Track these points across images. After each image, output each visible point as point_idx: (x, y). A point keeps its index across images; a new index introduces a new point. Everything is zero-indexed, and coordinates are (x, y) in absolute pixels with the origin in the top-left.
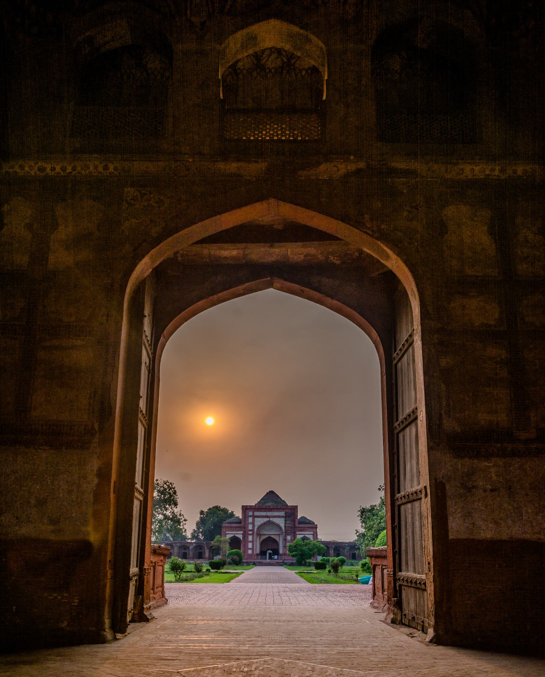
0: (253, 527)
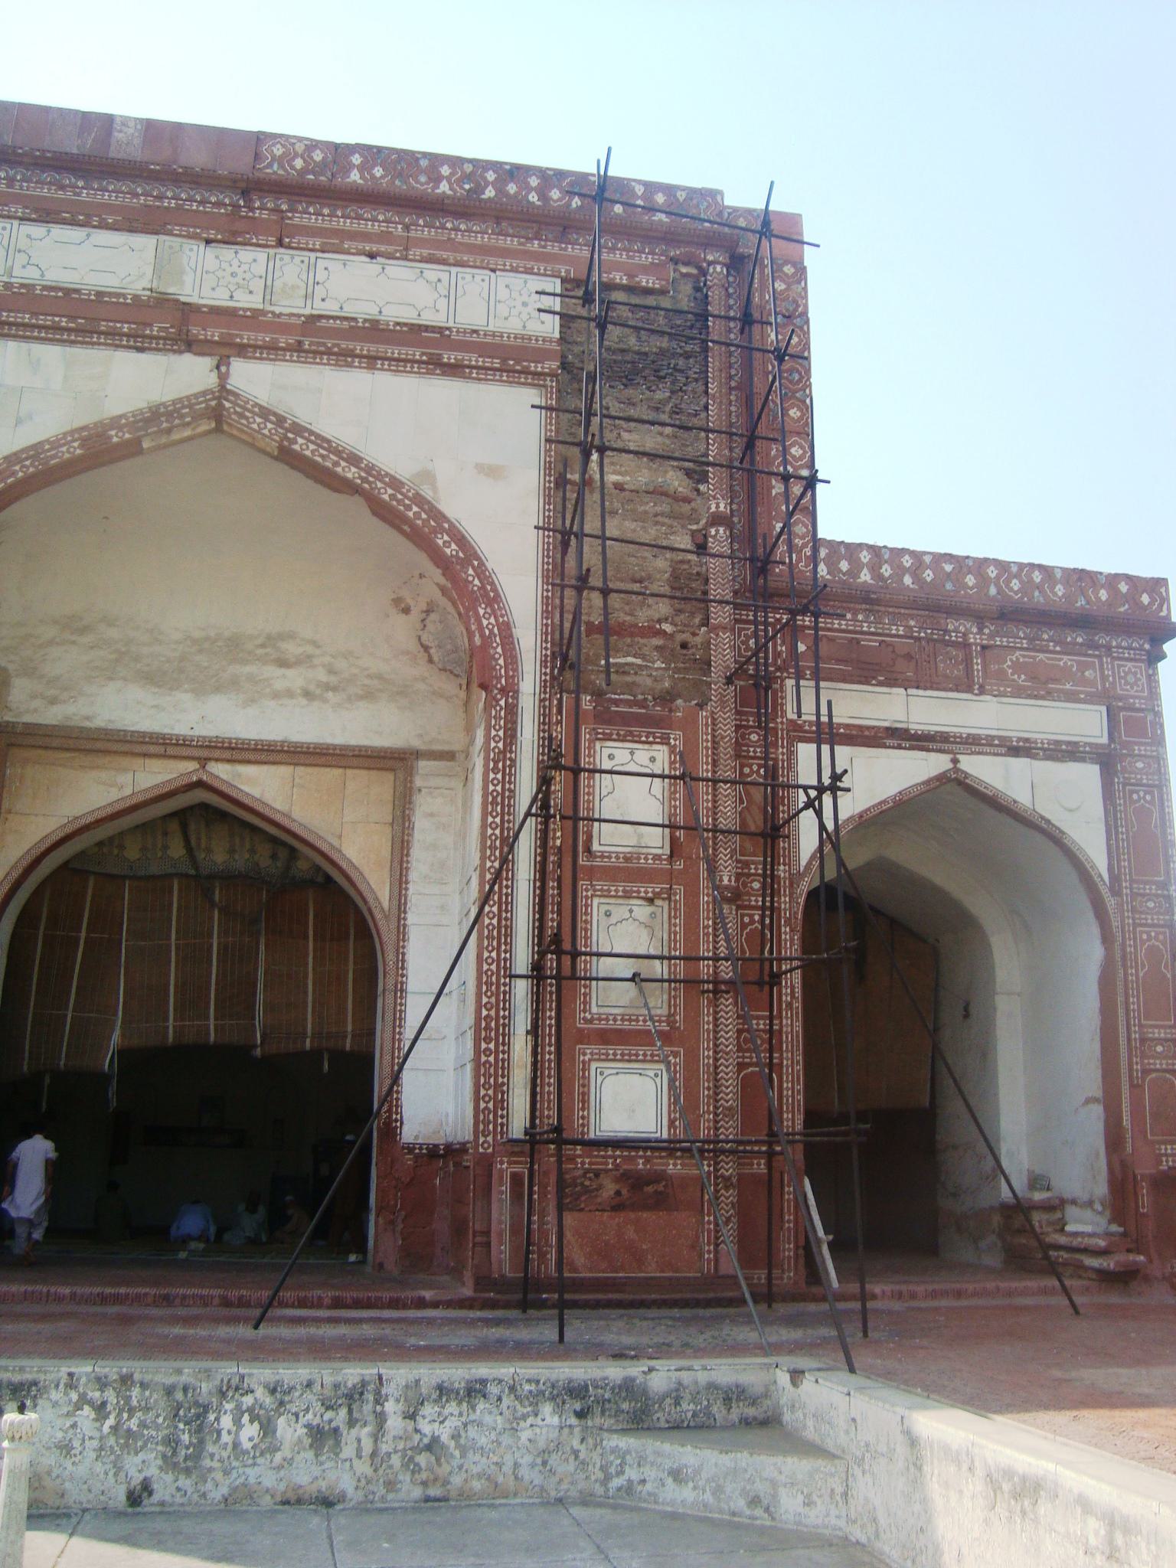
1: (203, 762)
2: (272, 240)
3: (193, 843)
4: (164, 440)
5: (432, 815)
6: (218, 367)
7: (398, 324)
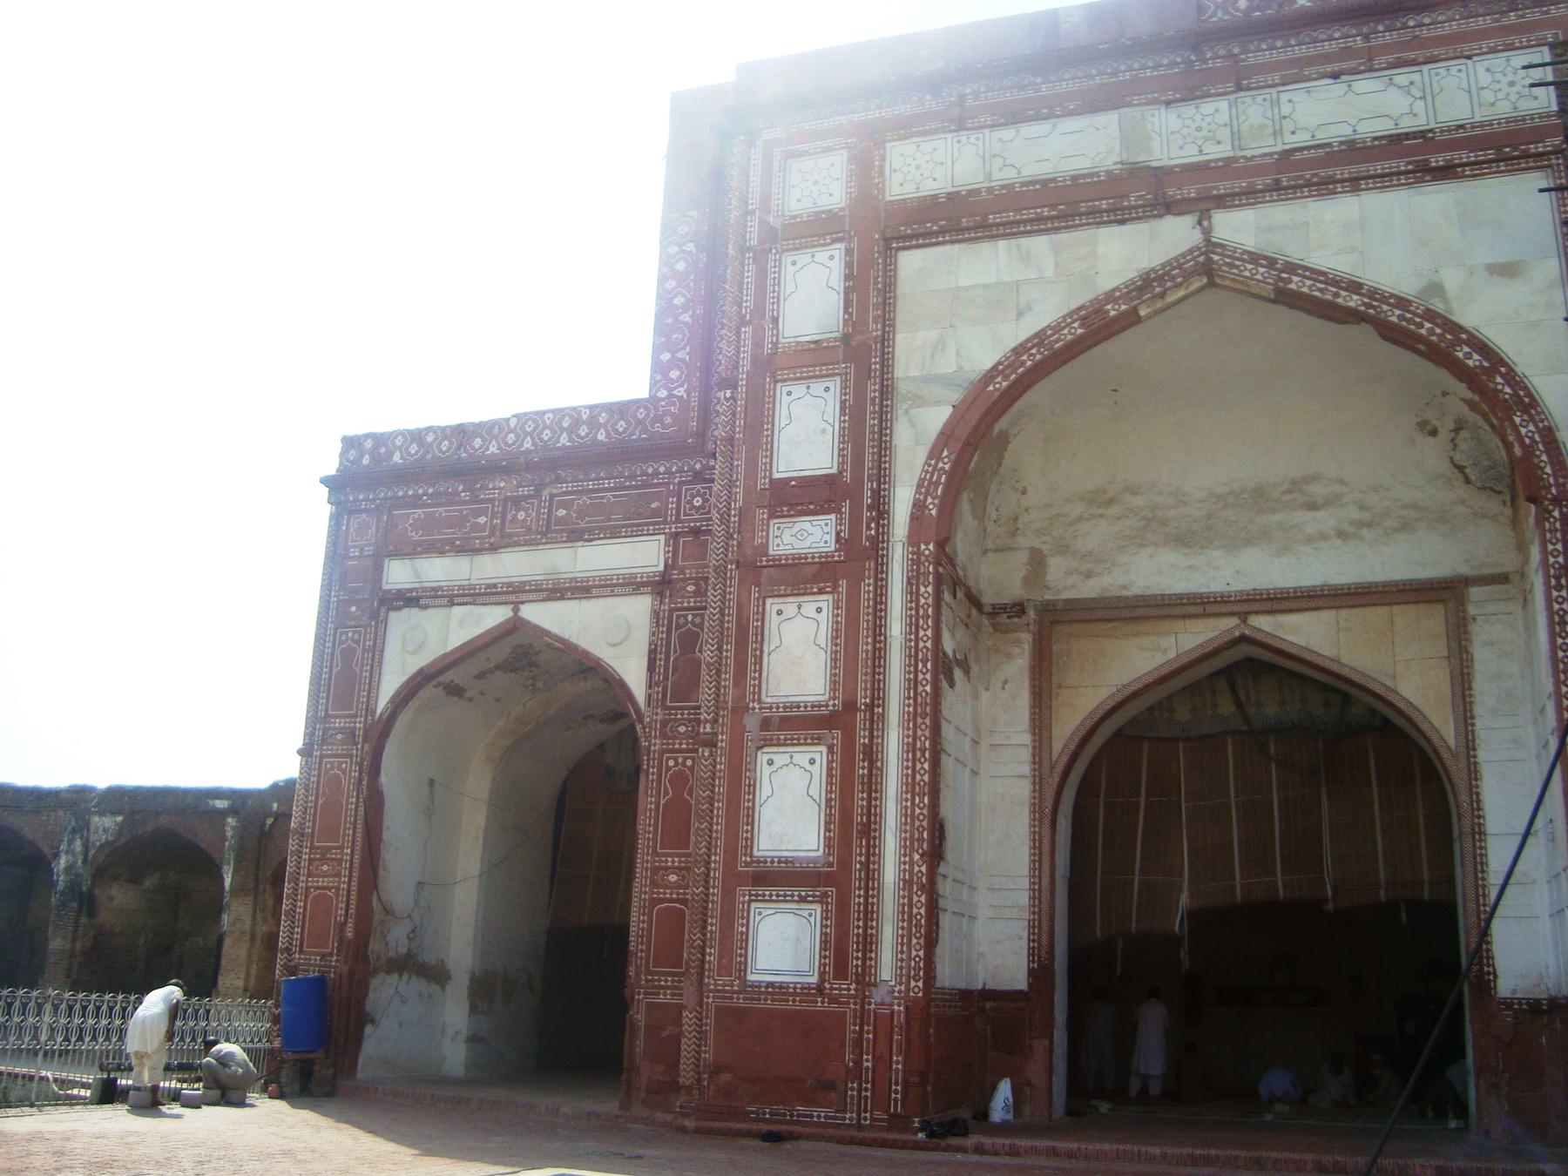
0: (867, 427)
1: (1243, 617)
2: (1230, 86)
3: (1243, 698)
4: (1159, 304)
5: (1492, 644)
6: (1200, 223)
7: (1376, 138)
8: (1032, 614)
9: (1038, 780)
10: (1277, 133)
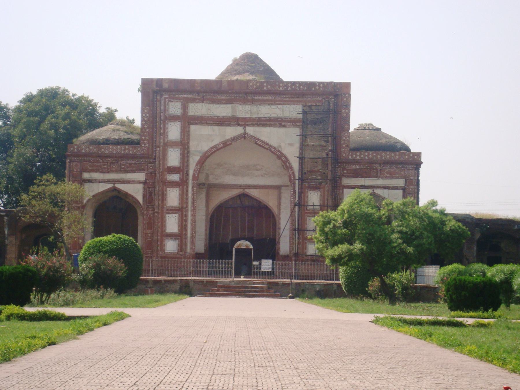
1: (244, 189)
8: (206, 186)
9: (207, 217)
10: (258, 114)
